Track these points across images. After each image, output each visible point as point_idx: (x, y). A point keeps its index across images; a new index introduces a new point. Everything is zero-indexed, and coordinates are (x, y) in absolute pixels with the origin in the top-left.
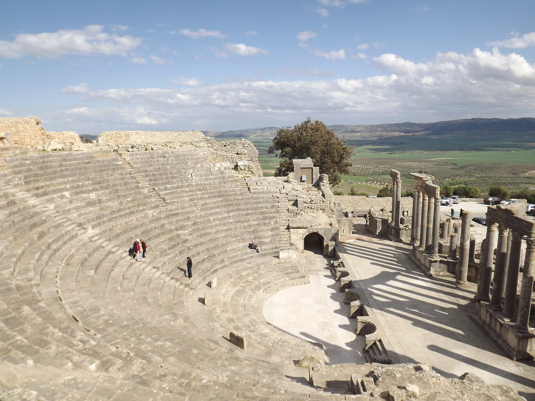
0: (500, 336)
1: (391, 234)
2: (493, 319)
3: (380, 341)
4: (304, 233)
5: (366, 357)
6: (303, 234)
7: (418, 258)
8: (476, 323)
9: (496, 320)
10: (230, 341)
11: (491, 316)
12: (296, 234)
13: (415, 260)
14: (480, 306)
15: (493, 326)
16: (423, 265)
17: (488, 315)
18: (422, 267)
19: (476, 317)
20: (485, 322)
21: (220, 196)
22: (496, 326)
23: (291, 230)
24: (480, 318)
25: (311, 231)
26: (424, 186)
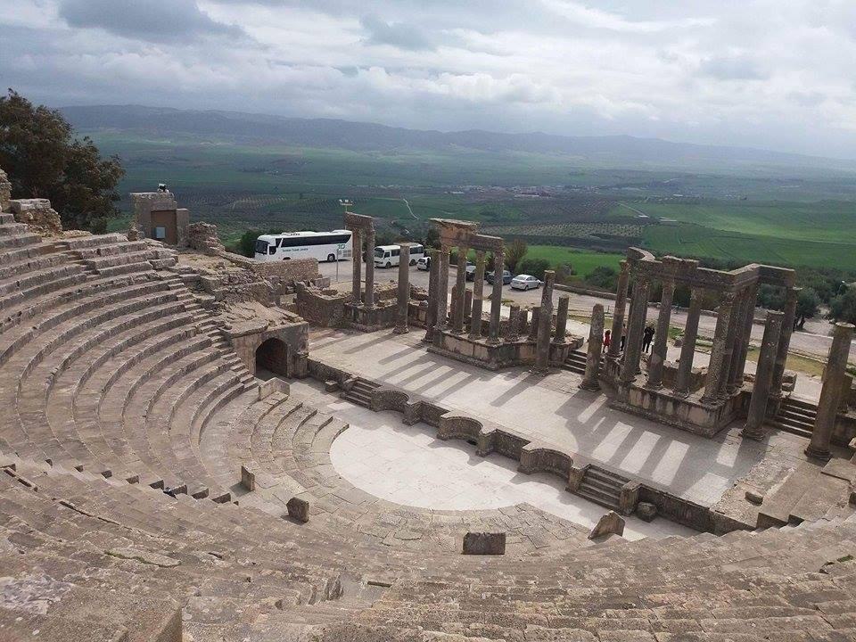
0: (675, 417)
1: (355, 320)
3: (591, 467)
4: (254, 341)
5: (585, 498)
6: (254, 346)
7: (451, 348)
8: (631, 412)
9: (665, 399)
10: (467, 551)
12: (242, 348)
15: (658, 409)
16: (469, 357)
17: (647, 397)
20: (640, 407)
21: (46, 290)
22: (665, 408)
23: (234, 340)
24: (629, 404)
25: (268, 336)
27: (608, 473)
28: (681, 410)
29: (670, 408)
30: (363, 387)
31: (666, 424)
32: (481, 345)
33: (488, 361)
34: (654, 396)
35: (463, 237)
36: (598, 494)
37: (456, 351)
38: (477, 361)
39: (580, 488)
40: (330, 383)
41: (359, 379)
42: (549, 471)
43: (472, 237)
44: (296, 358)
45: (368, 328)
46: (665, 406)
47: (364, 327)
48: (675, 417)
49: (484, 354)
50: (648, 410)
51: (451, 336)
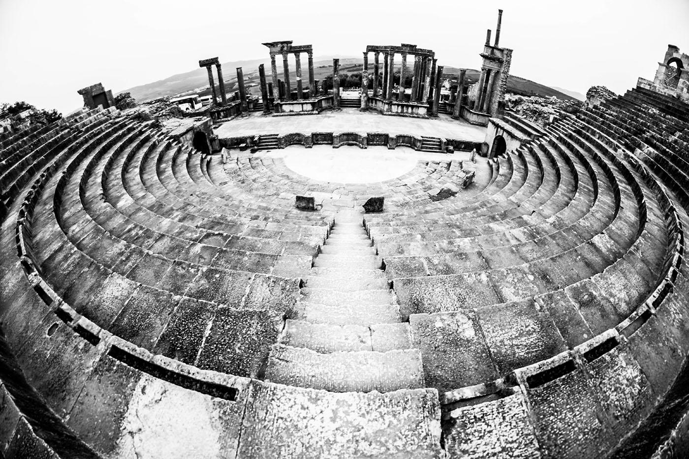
2: (405, 108)
6: (191, 139)
9: (408, 106)
11: (403, 106)
13: (286, 114)
14: (391, 106)
15: (405, 111)
17: (400, 107)
18: (302, 113)
19: (390, 113)
20: (397, 112)
27: (429, 138)
28: (414, 109)
29: (410, 109)
30: (266, 139)
31: (410, 117)
32: (307, 103)
33: (313, 110)
34: (403, 106)
35: (285, 49)
36: (430, 148)
37: (291, 111)
38: (306, 113)
39: (422, 148)
40: (242, 145)
41: (260, 136)
42: (400, 146)
43: (291, 47)
44: (213, 140)
45: (229, 119)
46: (408, 109)
47: (226, 119)
48: (412, 113)
49: (308, 107)
50: (401, 113)
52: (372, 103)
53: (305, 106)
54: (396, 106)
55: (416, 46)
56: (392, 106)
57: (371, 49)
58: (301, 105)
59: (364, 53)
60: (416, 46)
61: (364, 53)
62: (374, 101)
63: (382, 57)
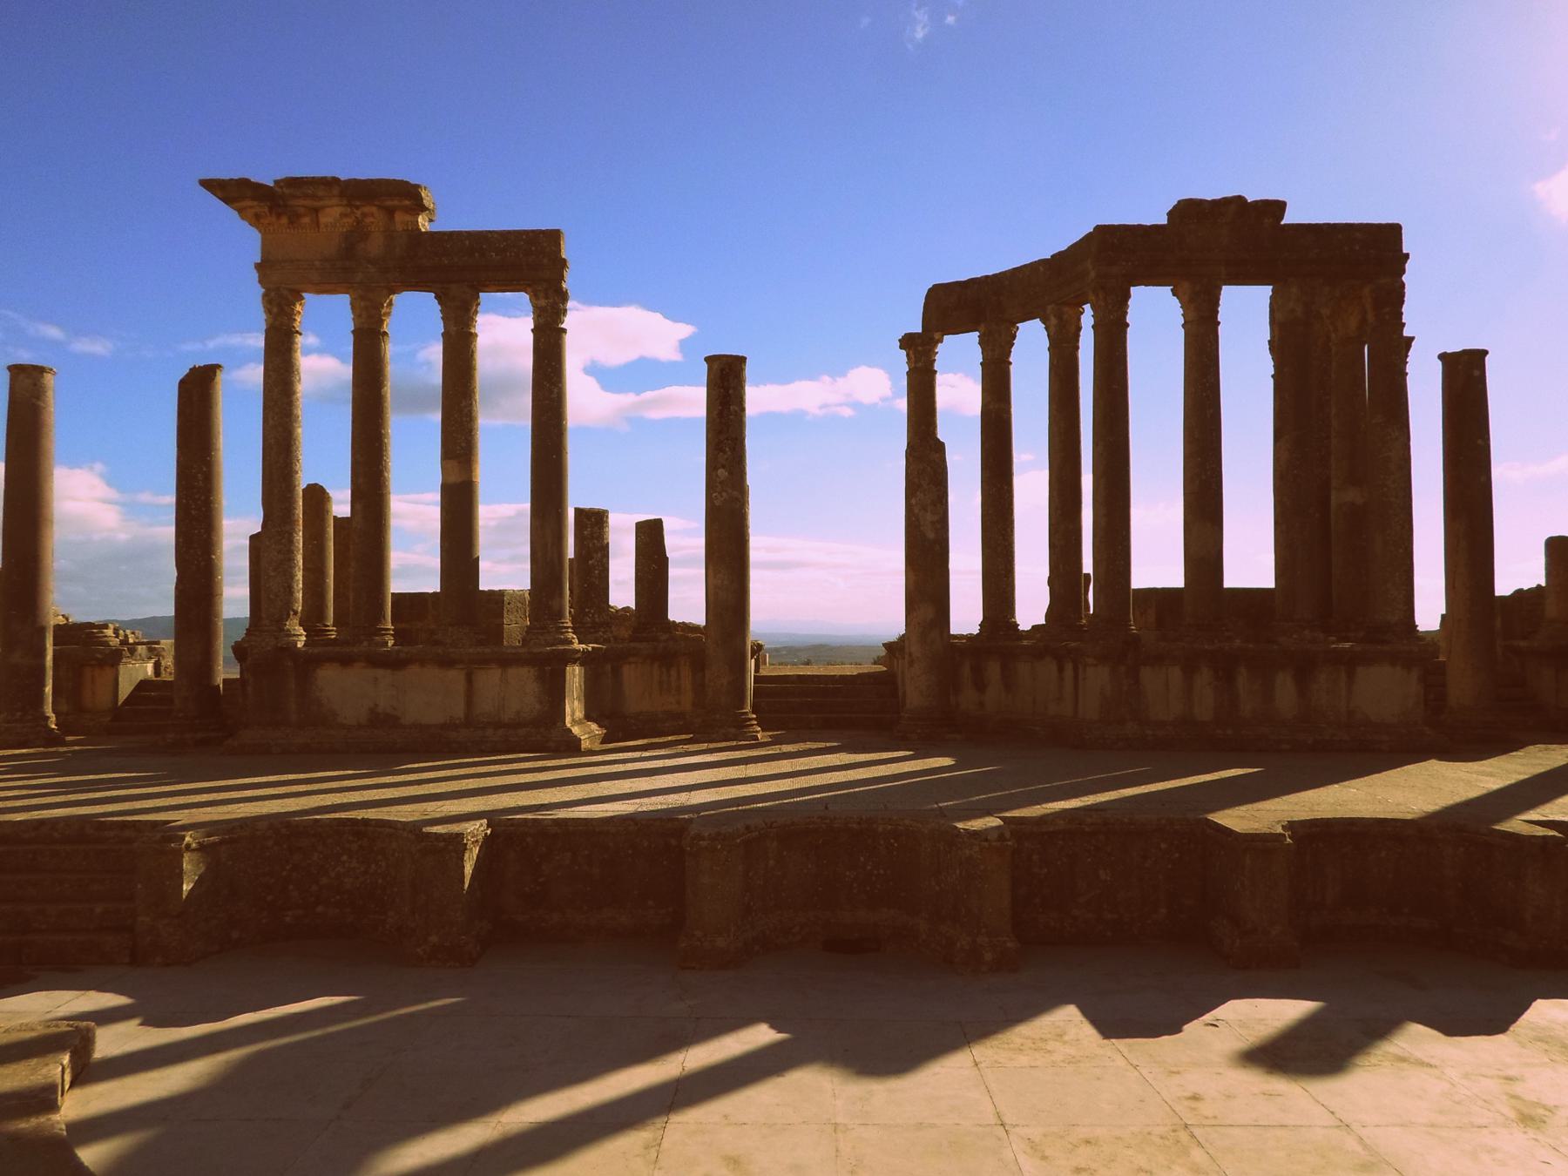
17: (1204, 677)
26: (375, 245)
29: (1285, 689)
35: (375, 245)
37: (381, 720)
51: (346, 661)
52: (980, 686)
53: (489, 679)
54: (1176, 673)
55: (1280, 207)
56: (1146, 674)
57: (952, 307)
58: (456, 676)
59: (908, 342)
60: (1280, 207)
61: (908, 342)
62: (993, 670)
63: (1031, 344)
